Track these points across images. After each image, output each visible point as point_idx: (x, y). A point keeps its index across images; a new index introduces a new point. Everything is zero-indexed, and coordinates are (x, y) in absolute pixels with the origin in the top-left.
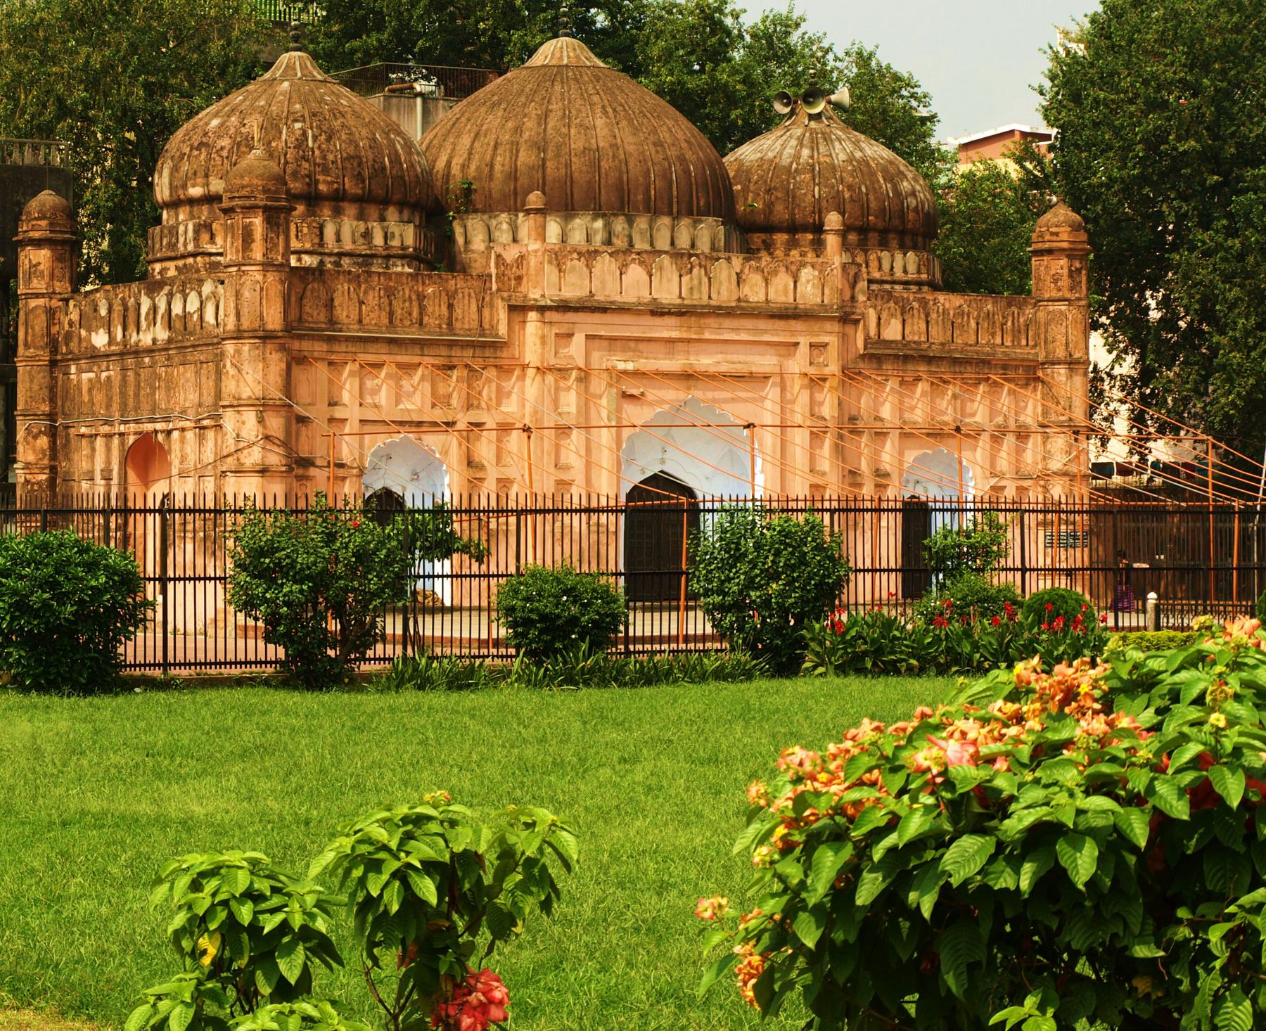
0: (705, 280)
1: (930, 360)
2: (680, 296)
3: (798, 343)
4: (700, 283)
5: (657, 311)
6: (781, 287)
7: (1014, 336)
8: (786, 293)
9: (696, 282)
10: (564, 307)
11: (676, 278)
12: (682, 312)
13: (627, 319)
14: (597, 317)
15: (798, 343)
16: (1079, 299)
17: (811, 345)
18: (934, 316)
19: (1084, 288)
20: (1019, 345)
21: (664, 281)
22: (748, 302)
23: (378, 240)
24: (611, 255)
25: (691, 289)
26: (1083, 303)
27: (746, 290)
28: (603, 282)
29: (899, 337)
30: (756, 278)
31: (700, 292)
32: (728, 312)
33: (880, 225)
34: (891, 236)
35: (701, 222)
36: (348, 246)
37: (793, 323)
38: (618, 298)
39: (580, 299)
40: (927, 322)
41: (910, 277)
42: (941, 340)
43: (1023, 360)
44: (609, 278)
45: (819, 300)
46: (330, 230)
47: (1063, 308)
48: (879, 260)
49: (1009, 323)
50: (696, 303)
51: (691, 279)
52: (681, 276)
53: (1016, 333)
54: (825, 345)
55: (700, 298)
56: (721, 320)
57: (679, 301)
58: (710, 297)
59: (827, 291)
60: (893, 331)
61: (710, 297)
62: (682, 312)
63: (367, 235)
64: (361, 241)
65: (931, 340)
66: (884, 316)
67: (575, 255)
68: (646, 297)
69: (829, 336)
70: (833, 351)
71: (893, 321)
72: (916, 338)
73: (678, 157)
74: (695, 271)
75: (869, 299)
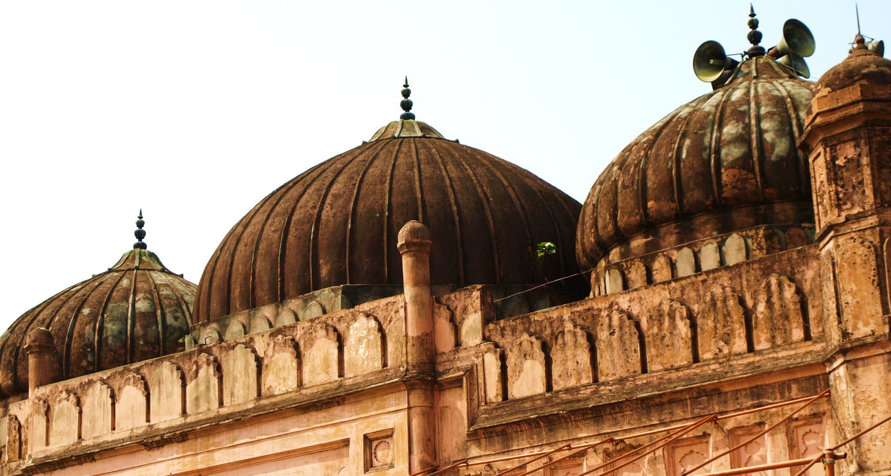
0: (215, 381)
1: (597, 414)
2: (184, 412)
3: (346, 443)
4: (208, 388)
6: (319, 361)
7: (773, 329)
8: (327, 366)
9: (202, 388)
11: (178, 390)
12: (181, 436)
15: (346, 443)
16: (859, 217)
17: (368, 441)
18: (603, 335)
19: (869, 192)
20: (788, 343)
21: (164, 395)
22: (273, 396)
24: (103, 382)
25: (197, 399)
26: (872, 220)
27: (270, 380)
28: (93, 421)
29: (540, 388)
30: (285, 358)
31: (208, 401)
33: (668, 207)
34: (700, 220)
35: (313, 297)
37: (337, 410)
38: (110, 437)
39: (68, 450)
40: (593, 351)
42: (620, 373)
43: (788, 370)
44: (99, 413)
45: (378, 365)
47: (831, 245)
49: (761, 307)
50: (201, 417)
51: (197, 385)
52: (184, 386)
53: (778, 324)
54: (387, 435)
55: (206, 408)
56: (236, 433)
58: (221, 404)
59: (390, 348)
60: (528, 381)
61: (221, 404)
62: (181, 436)
65: (602, 379)
66: (511, 360)
67: (64, 395)
68: (140, 425)
69: (394, 416)
70: (400, 441)
71: (528, 363)
72: (572, 383)
73: (300, 222)
74: (202, 373)
75: (485, 339)
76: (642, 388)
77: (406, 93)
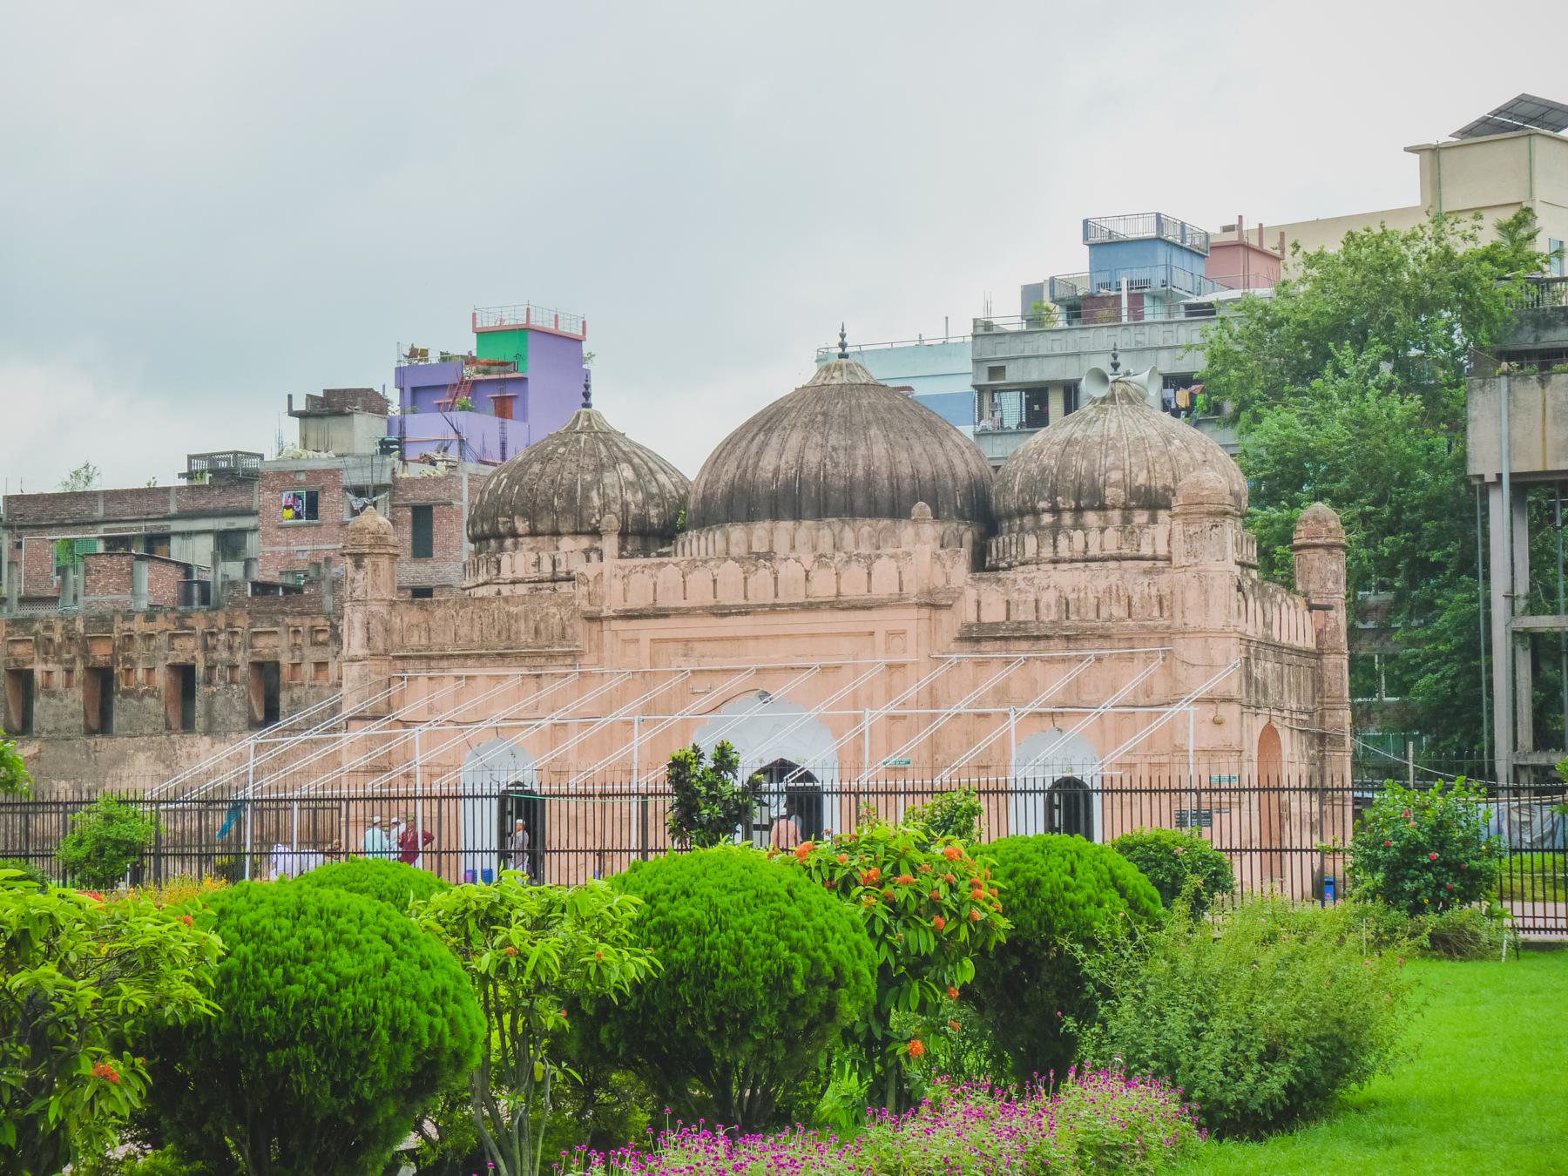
2: (746, 597)
5: (721, 612)
10: (628, 616)
13: (692, 622)
14: (661, 622)
15: (872, 634)
23: (547, 568)
29: (1002, 618)
32: (793, 607)
36: (520, 574)
38: (683, 604)
41: (1107, 552)
46: (505, 560)
48: (1070, 539)
57: (743, 602)
58: (776, 595)
60: (994, 613)
61: (776, 595)
63: (538, 563)
64: (533, 569)
68: (710, 601)
74: (762, 572)
76: (1067, 628)
77: (843, 336)
